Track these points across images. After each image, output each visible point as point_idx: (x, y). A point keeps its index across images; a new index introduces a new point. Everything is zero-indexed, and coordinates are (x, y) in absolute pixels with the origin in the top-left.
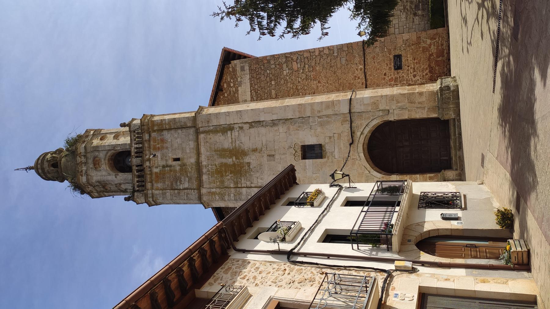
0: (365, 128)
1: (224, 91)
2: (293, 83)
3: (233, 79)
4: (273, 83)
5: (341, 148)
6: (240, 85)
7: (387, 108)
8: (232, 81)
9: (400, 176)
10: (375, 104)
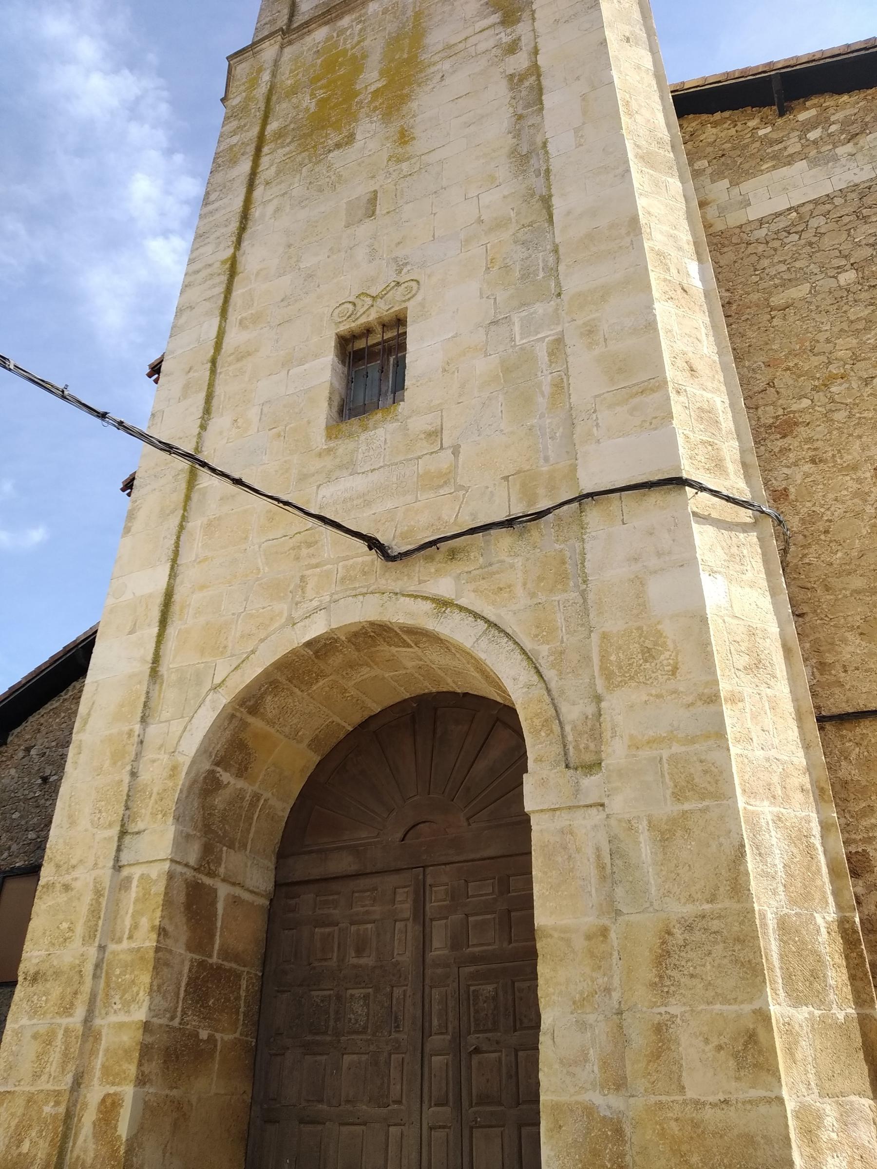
0: (484, 628)
1: (780, 121)
2: (856, 359)
3: (842, 131)
4: (848, 277)
5: (368, 504)
6: (814, 163)
7: (616, 753)
8: (833, 128)
9: (158, 872)
10: (648, 654)
